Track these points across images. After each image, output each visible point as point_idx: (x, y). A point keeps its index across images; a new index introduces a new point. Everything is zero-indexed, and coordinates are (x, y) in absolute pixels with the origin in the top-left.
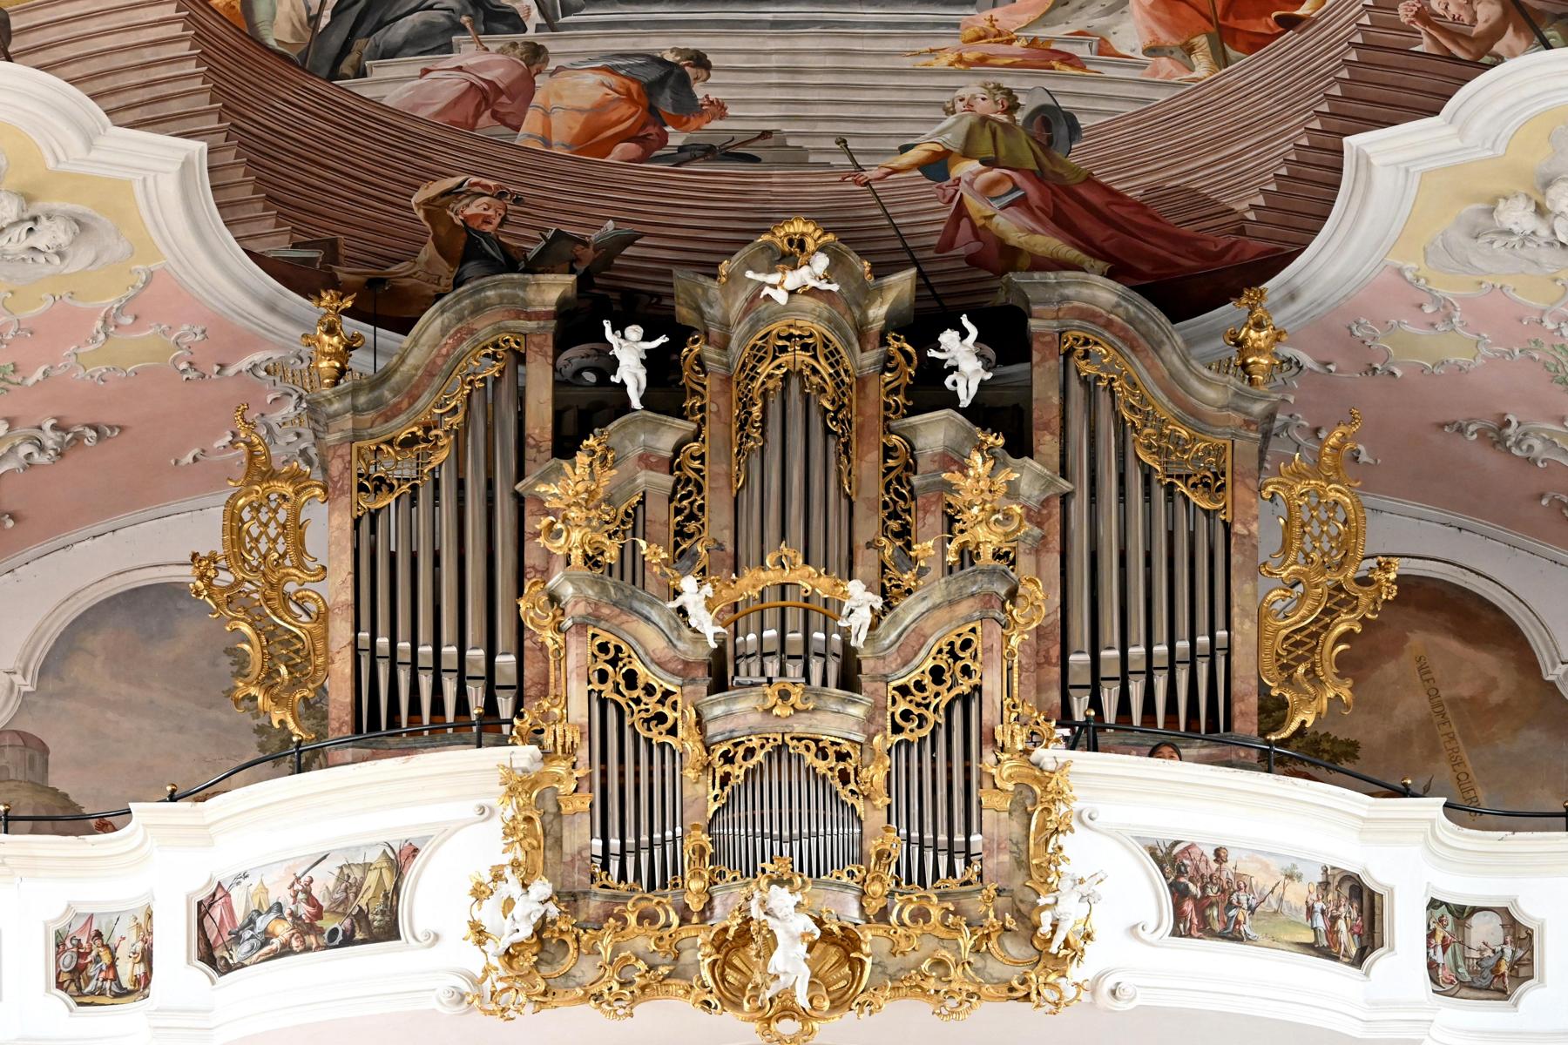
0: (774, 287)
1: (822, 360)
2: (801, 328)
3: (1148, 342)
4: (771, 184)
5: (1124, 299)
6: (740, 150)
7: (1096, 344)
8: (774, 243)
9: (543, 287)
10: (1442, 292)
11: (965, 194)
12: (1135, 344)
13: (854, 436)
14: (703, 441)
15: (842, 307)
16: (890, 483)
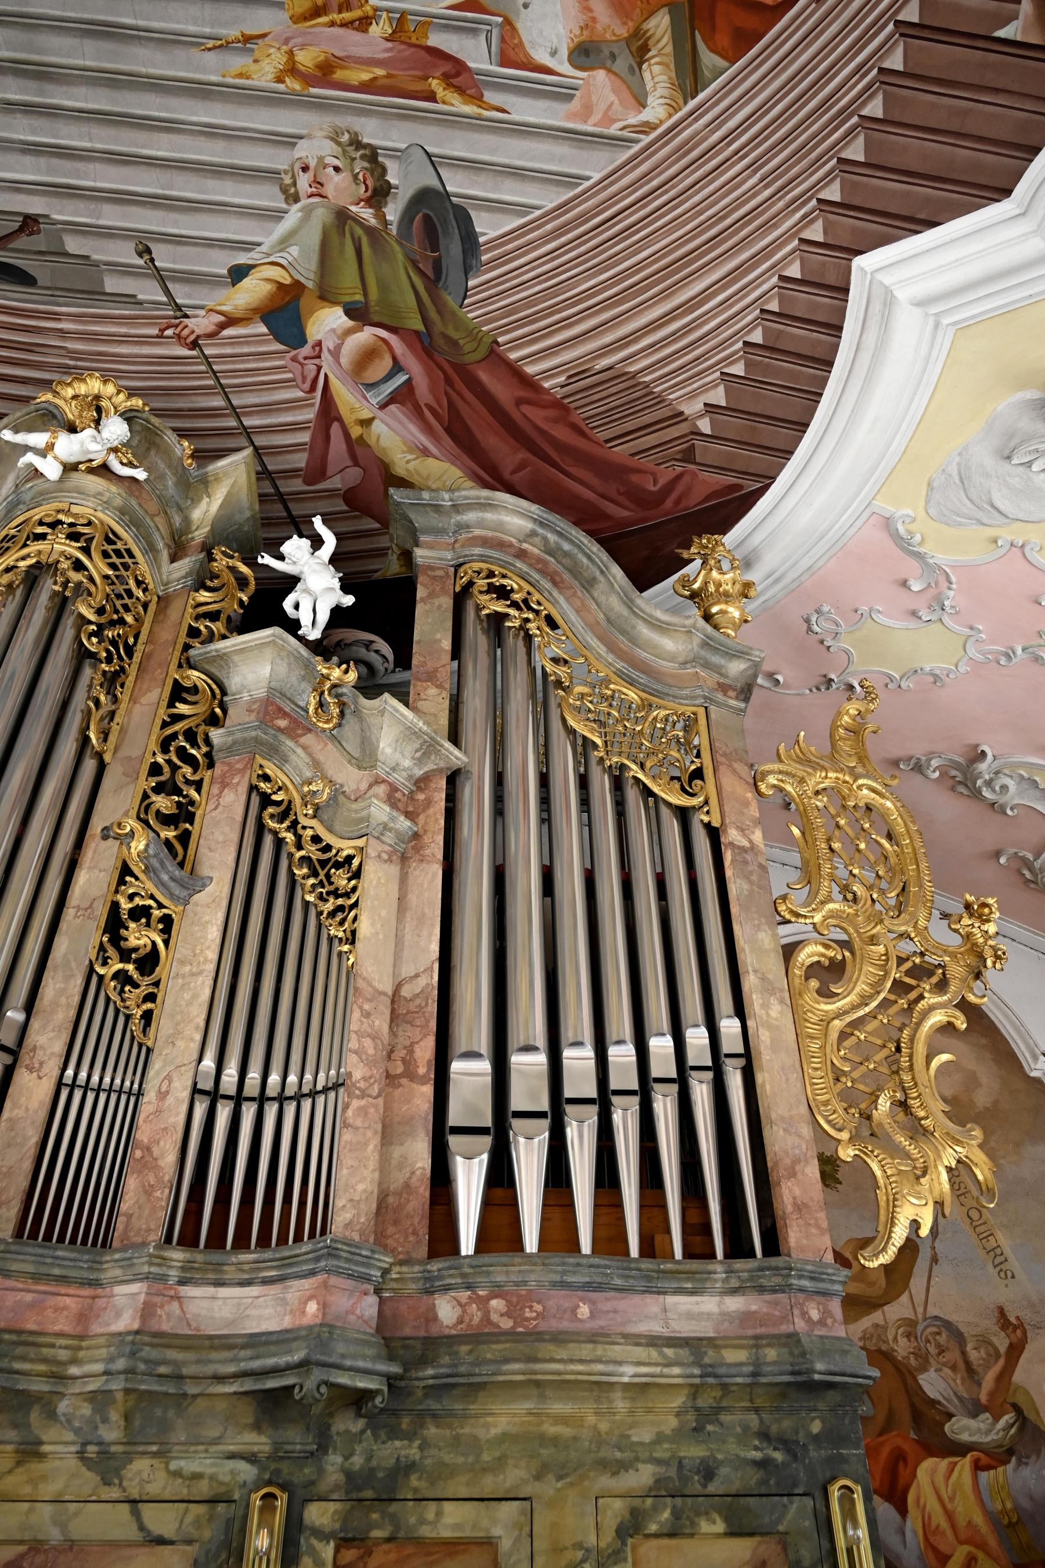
0: (43, 453)
1: (96, 555)
2: (76, 516)
3: (575, 577)
4: (62, 333)
5: (542, 524)
7: (504, 576)
8: (57, 407)
10: (940, 557)
11: (331, 376)
12: (557, 579)
15: (153, 506)
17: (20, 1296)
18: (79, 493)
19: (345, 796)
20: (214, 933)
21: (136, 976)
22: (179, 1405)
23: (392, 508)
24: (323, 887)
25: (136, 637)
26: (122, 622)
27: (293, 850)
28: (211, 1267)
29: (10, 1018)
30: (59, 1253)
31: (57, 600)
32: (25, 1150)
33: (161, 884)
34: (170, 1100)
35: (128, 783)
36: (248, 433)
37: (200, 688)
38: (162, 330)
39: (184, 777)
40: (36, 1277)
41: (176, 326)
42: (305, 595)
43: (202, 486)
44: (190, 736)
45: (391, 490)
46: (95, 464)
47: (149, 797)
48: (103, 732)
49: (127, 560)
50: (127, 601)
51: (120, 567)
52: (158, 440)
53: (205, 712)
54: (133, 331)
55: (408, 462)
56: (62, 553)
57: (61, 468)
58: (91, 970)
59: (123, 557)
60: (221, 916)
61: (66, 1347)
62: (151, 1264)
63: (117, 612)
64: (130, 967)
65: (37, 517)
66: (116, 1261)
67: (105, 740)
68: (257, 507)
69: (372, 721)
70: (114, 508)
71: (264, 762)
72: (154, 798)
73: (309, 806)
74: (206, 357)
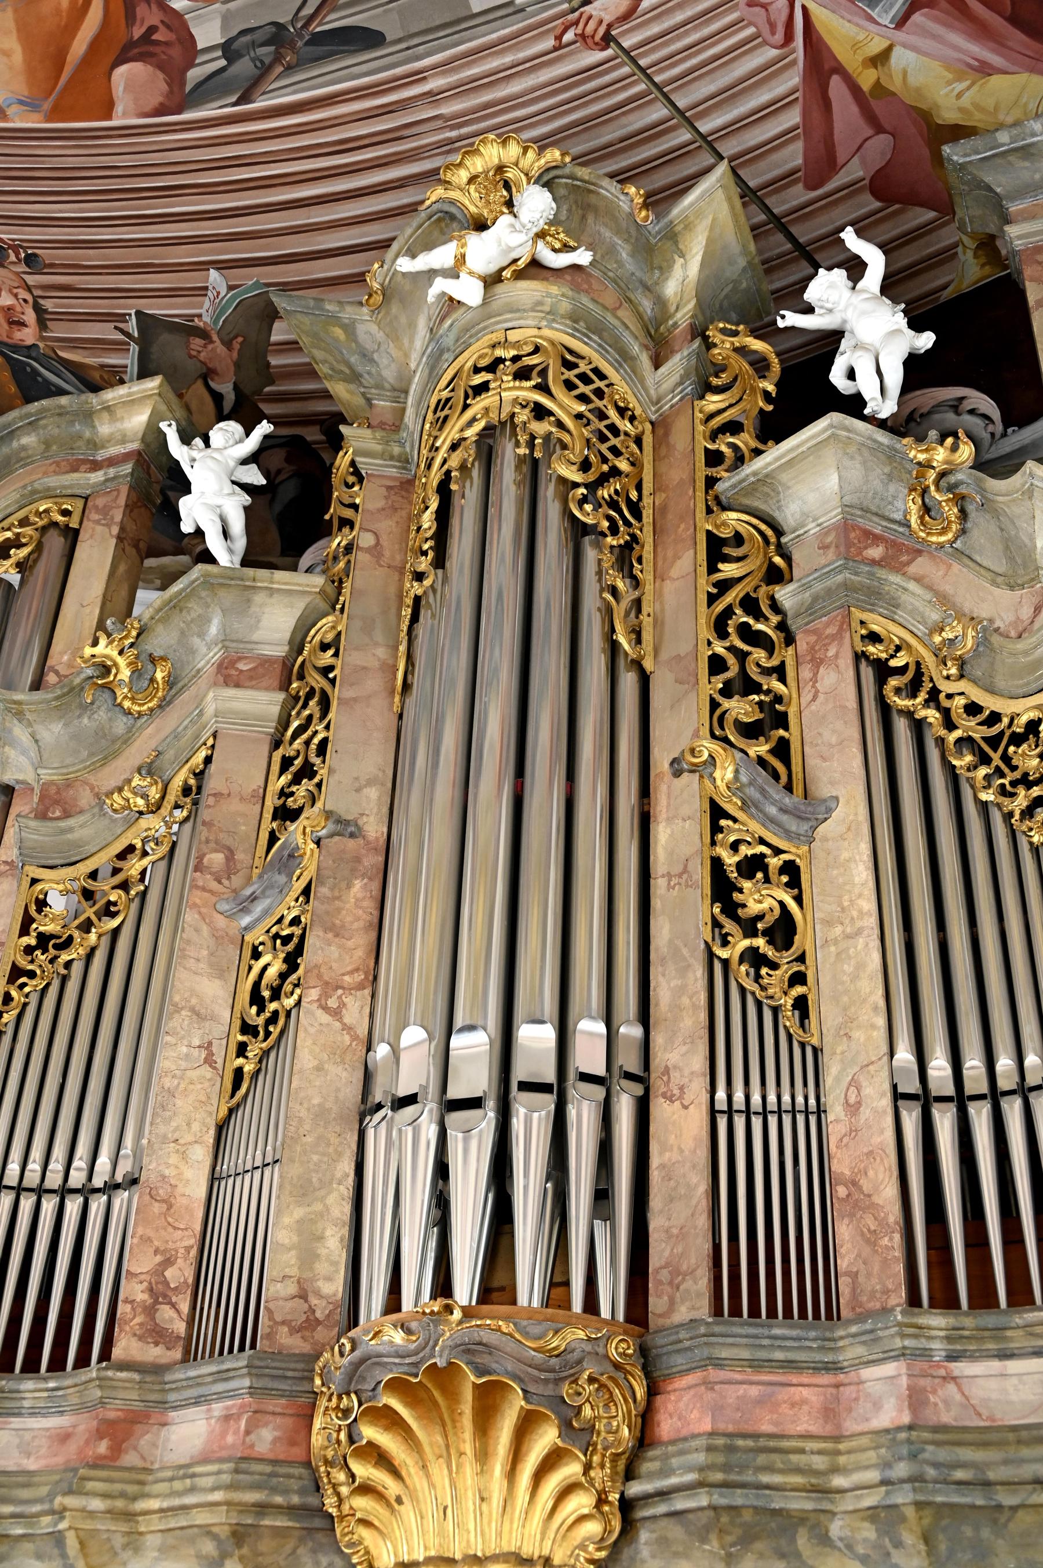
0: (453, 273)
1: (557, 390)
2: (517, 345)
6: (333, 21)
8: (452, 202)
9: (120, 412)
13: (647, 536)
14: (342, 610)
15: (610, 298)
16: (728, 612)
17: (742, 1390)
18: (511, 312)
19: (1001, 634)
20: (863, 874)
21: (770, 952)
22: (995, 1522)
23: (953, 178)
24: (1003, 775)
25: (639, 488)
26: (615, 472)
27: (942, 732)
28: (987, 1334)
29: (626, 1037)
30: (777, 1331)
31: (526, 469)
32: (694, 1202)
33: (768, 821)
34: (865, 1113)
35: (686, 692)
36: (708, 142)
37: (745, 535)
38: (559, 38)
39: (758, 665)
40: (756, 1365)
41: (576, 23)
42: (859, 353)
43: (669, 244)
44: (750, 605)
45: (946, 149)
46: (521, 264)
47: (719, 705)
48: (633, 631)
49: (599, 384)
50: (614, 441)
51: (593, 397)
52: (593, 199)
53: (760, 567)
54: (521, 55)
55: (959, 96)
56: (515, 401)
57: (482, 284)
58: (711, 956)
59: (592, 382)
60: (865, 848)
61: (820, 1452)
62: (903, 1336)
63: (605, 460)
64: (760, 942)
65: (470, 364)
66: (854, 1336)
67: (639, 641)
68: (752, 247)
69: (1016, 510)
70: (563, 317)
71: (865, 616)
72: (726, 704)
73: (949, 664)
74: (626, 52)
